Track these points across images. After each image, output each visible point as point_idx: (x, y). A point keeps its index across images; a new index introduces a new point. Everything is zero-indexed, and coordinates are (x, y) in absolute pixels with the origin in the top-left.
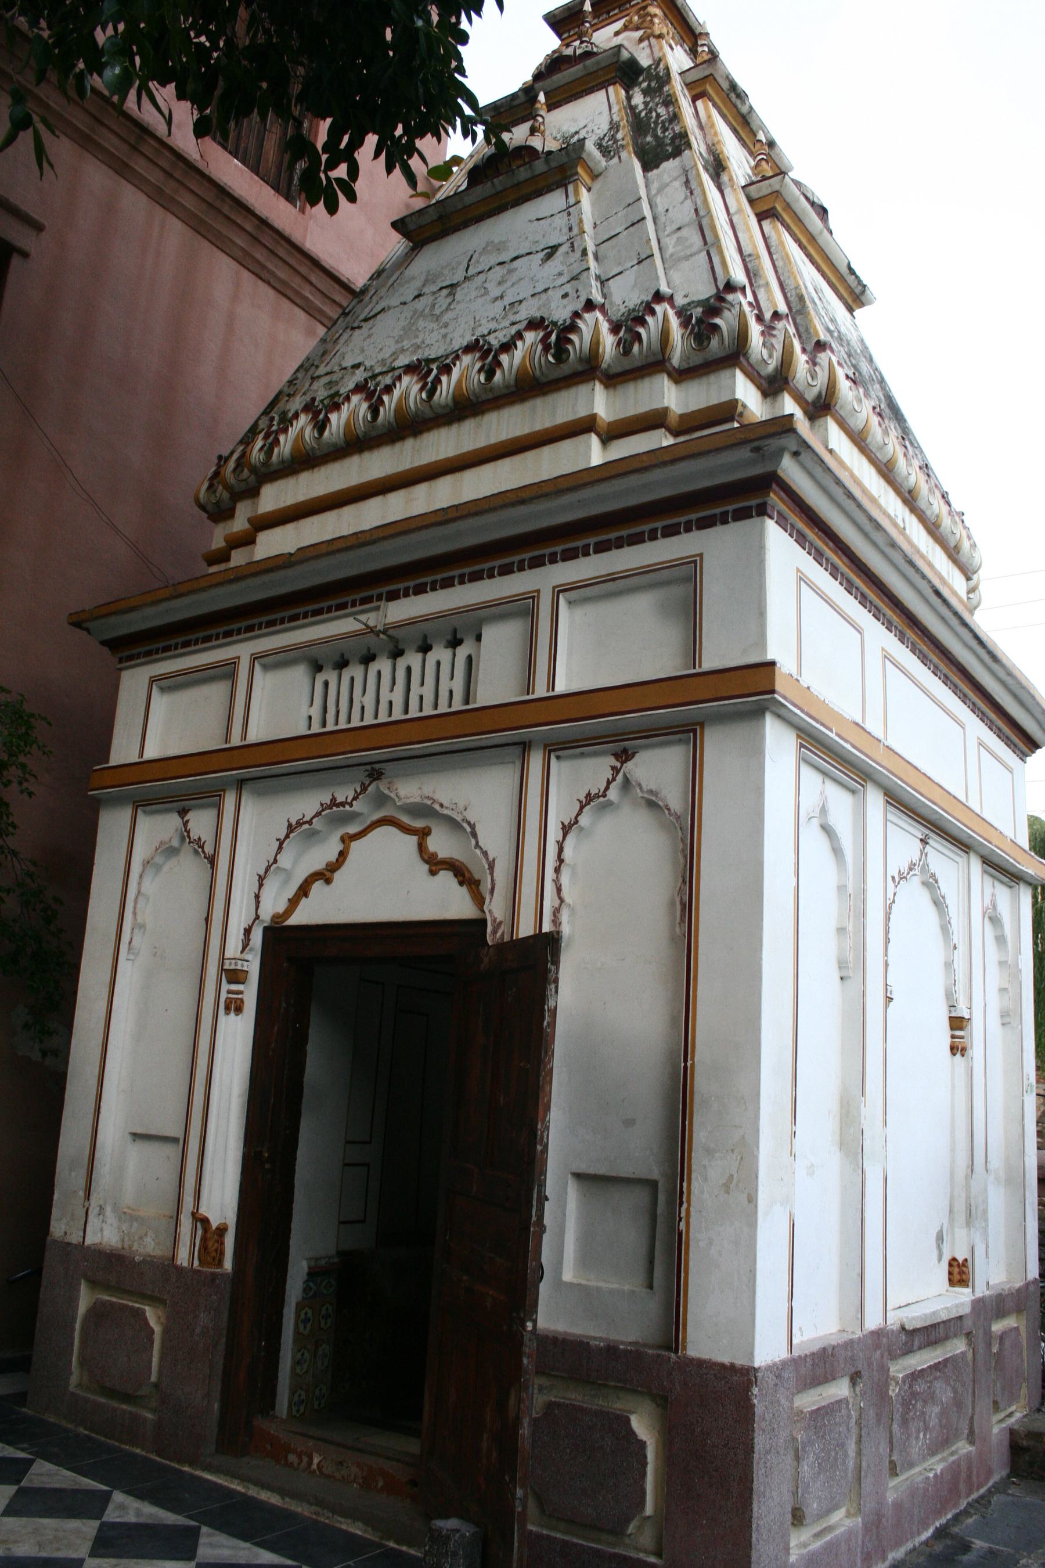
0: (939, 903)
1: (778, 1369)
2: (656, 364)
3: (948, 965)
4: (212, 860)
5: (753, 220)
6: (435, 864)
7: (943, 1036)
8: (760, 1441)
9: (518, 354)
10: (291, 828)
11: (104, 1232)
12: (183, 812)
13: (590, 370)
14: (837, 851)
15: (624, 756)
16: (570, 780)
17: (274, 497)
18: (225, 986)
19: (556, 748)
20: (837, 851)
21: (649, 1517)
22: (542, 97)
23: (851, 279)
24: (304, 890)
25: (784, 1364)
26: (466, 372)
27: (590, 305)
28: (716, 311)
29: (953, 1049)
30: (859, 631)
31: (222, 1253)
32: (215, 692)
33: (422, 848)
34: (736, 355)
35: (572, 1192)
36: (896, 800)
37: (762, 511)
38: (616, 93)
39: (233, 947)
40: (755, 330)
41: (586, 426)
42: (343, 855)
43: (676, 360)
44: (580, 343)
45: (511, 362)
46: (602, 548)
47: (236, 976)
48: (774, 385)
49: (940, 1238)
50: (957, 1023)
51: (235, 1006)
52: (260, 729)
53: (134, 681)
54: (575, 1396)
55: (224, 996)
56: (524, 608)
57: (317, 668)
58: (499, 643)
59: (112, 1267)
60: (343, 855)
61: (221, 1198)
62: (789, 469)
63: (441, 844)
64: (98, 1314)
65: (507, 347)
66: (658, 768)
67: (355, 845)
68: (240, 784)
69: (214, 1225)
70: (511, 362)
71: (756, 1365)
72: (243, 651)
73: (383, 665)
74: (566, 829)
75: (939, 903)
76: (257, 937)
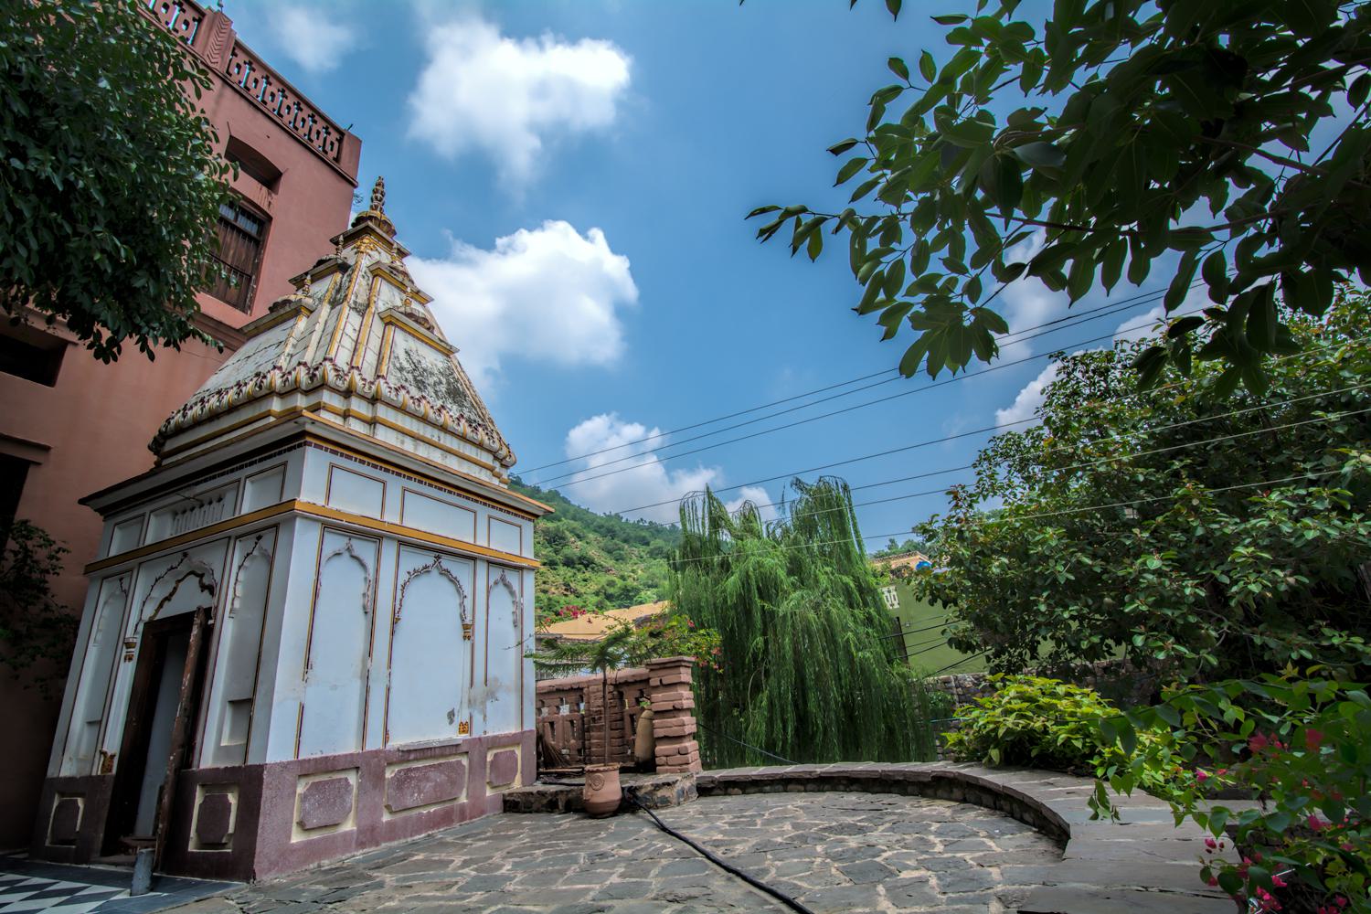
0: (454, 581)
1: (285, 766)
3: (462, 604)
4: (127, 596)
5: (382, 326)
6: (203, 587)
9: (249, 386)
10: (157, 581)
12: (121, 579)
14: (363, 565)
15: (259, 538)
18: (125, 650)
20: (363, 565)
21: (231, 834)
22: (309, 277)
23: (443, 344)
24: (161, 606)
25: (289, 763)
26: (231, 396)
28: (317, 369)
29: (465, 637)
30: (384, 483)
31: (112, 766)
33: (200, 581)
36: (401, 543)
37: (306, 444)
38: (338, 276)
39: (130, 633)
40: (331, 376)
41: (268, 414)
42: (175, 589)
43: (304, 387)
46: (261, 460)
47: (129, 645)
48: (348, 393)
49: (451, 715)
50: (466, 627)
55: (124, 654)
57: (176, 514)
58: (229, 498)
60: (175, 589)
61: (113, 742)
62: (309, 428)
63: (206, 581)
65: (246, 384)
67: (180, 585)
68: (140, 564)
69: (109, 754)
71: (268, 761)
73: (197, 510)
74: (240, 567)
75: (454, 581)
76: (141, 627)
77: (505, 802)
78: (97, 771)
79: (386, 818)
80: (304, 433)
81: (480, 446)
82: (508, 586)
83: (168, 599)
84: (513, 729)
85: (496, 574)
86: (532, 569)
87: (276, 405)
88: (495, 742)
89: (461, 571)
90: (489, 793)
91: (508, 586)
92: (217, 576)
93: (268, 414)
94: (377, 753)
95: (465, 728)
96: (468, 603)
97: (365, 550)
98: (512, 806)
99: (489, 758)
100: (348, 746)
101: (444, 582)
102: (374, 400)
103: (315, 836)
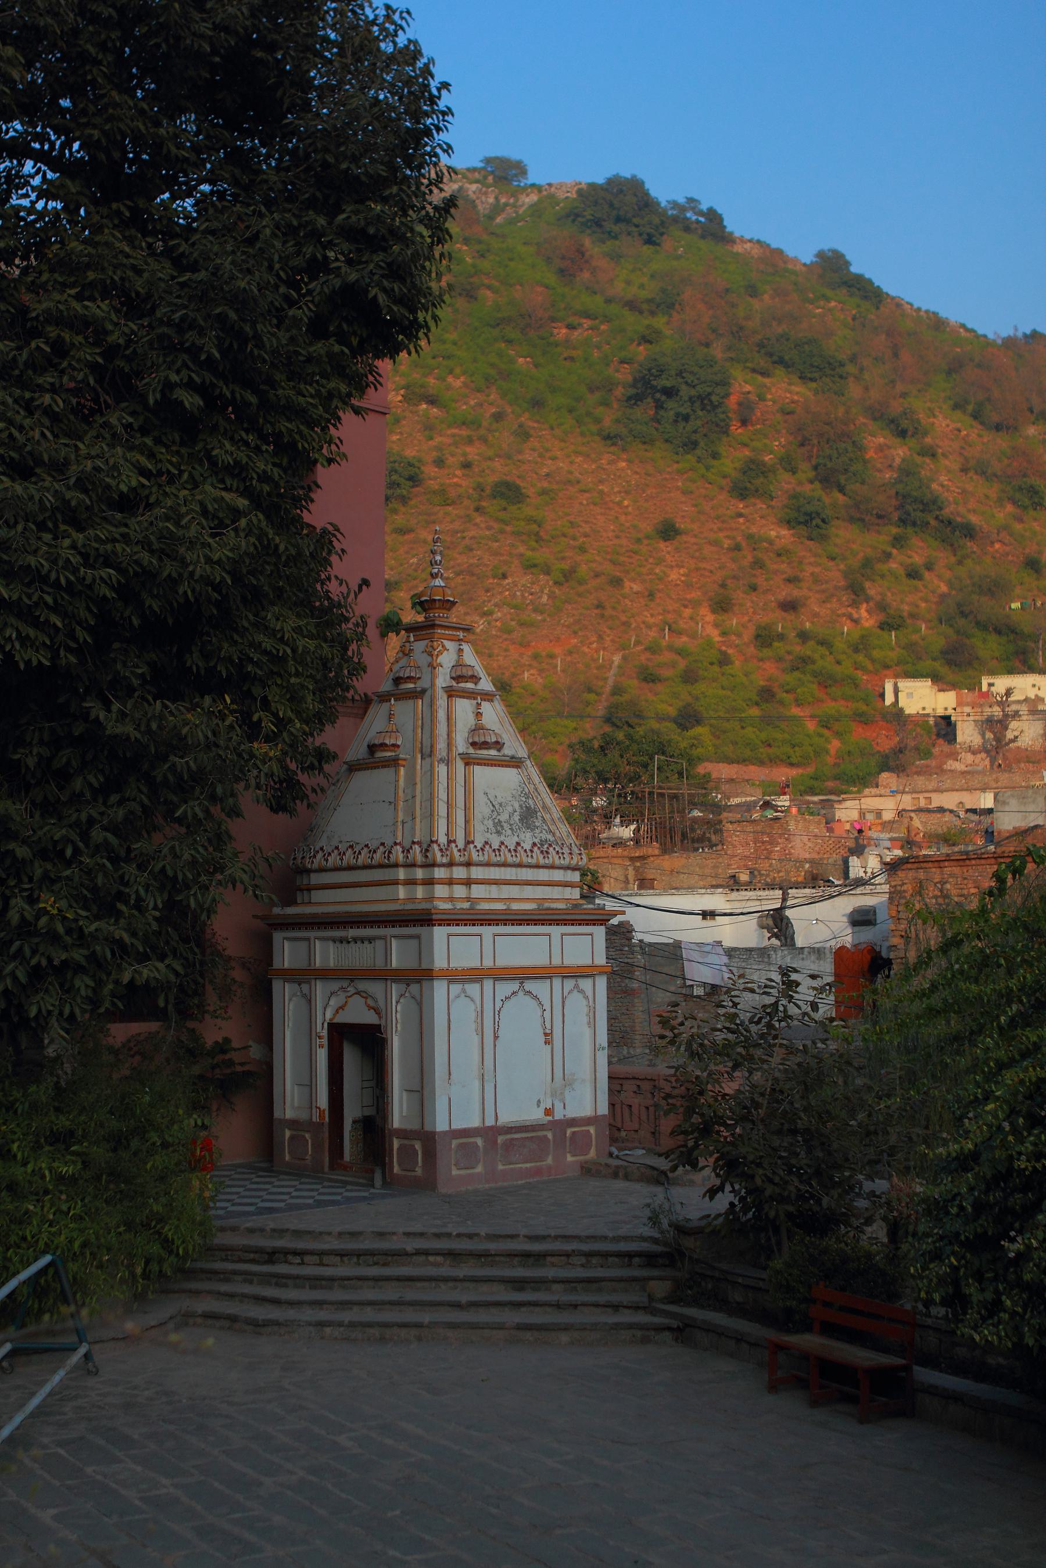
0: (536, 998)
1: (445, 1133)
2: (414, 865)
6: (370, 1008)
7: (543, 1038)
8: (438, 1147)
11: (289, 1114)
13: (396, 865)
16: (395, 989)
17: (315, 879)
19: (394, 981)
27: (396, 844)
32: (304, 945)
34: (434, 865)
35: (405, 1094)
39: (319, 1029)
41: (396, 882)
44: (393, 858)
45: (378, 857)
50: (546, 1034)
51: (321, 1046)
52: (318, 963)
53: (278, 936)
54: (406, 1142)
56: (383, 938)
59: (294, 1124)
61: (323, 1101)
62: (434, 917)
63: (370, 1001)
64: (292, 1138)
66: (414, 988)
70: (378, 857)
72: (312, 934)
75: (536, 998)
77: (582, 1167)
78: (315, 1119)
79: (501, 1167)
80: (431, 920)
81: (552, 867)
82: (581, 991)
83: (342, 1008)
84: (587, 1111)
85: (569, 984)
86: (601, 973)
87: (402, 874)
88: (573, 1122)
89: (540, 988)
90: (570, 1158)
91: (581, 991)
92: (381, 1004)
93: (396, 882)
94: (491, 1128)
95: (548, 1112)
96: (547, 1014)
97: (473, 989)
98: (588, 1170)
99: (569, 1131)
100: (476, 1123)
101: (528, 998)
102: (468, 864)
103: (463, 1172)
